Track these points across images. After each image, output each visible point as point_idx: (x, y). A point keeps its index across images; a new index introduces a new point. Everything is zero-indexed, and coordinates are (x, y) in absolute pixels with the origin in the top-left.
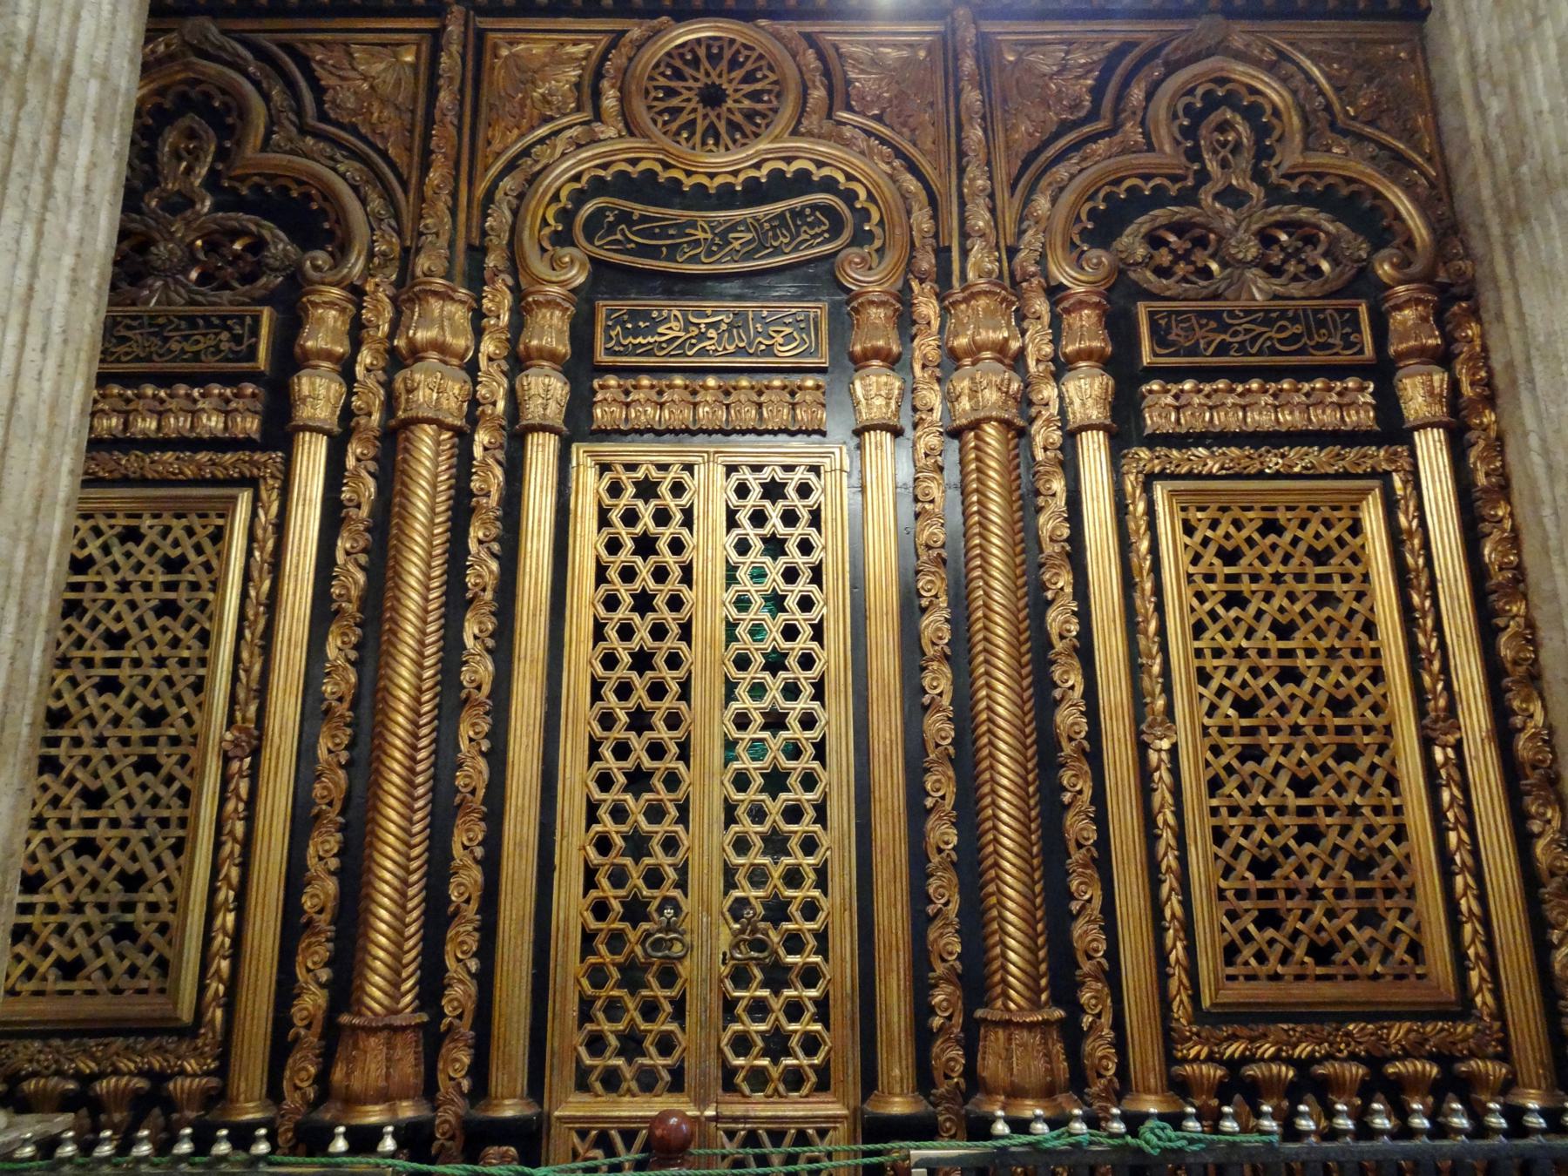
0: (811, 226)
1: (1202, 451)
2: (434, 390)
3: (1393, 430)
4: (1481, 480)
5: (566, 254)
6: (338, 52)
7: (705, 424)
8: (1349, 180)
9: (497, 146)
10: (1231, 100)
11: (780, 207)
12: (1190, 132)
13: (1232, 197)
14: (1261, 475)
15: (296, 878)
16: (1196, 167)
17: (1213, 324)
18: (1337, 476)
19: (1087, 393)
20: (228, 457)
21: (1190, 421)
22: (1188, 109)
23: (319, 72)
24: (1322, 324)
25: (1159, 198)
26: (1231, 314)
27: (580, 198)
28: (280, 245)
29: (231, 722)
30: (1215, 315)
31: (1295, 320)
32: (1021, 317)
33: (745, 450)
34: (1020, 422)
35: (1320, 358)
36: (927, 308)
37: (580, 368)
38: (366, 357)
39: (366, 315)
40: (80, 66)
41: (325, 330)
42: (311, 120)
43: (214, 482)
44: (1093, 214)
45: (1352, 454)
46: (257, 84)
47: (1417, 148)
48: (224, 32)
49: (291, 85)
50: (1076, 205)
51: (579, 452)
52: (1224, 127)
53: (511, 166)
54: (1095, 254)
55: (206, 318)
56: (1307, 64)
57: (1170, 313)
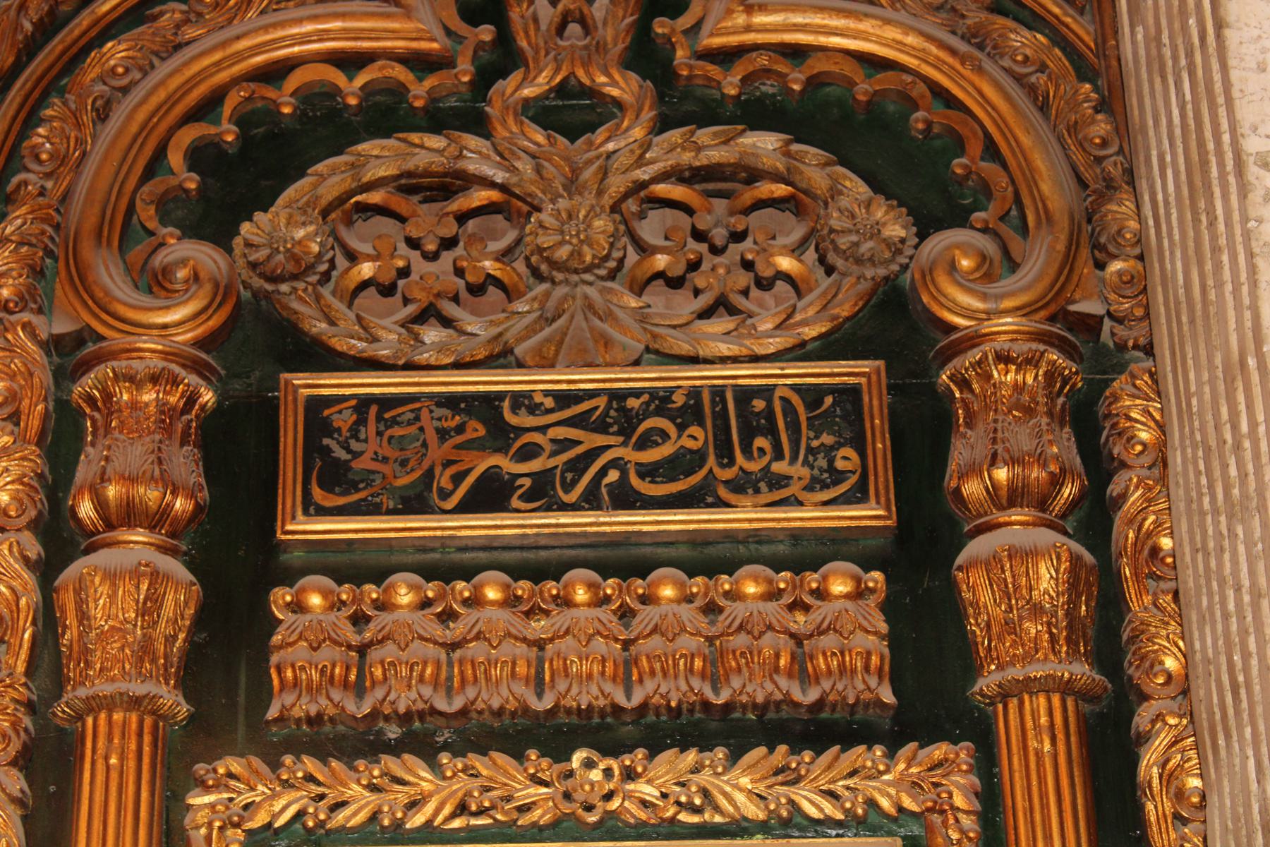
16: (486, 33)
17: (476, 429)
25: (386, 115)
26: (521, 401)
30: (486, 405)
54: (188, 254)
57: (364, 403)
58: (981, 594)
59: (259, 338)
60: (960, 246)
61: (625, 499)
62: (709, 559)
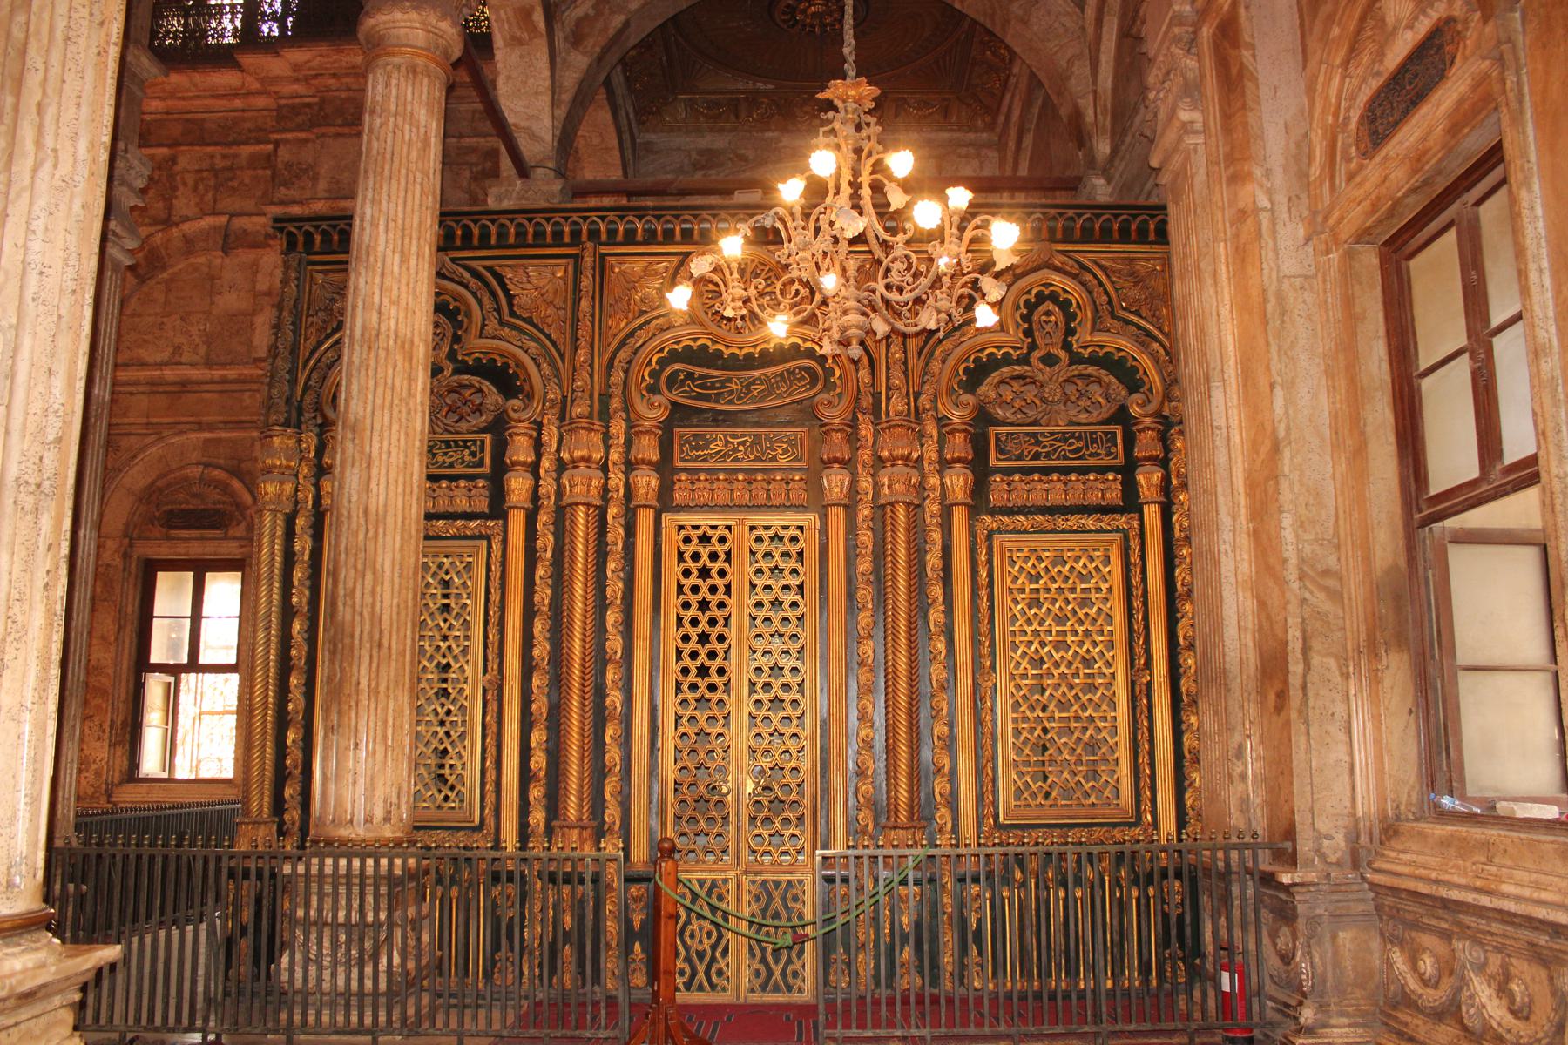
0: (799, 380)
1: (1021, 518)
2: (583, 485)
3: (1131, 503)
4: (1177, 534)
5: (657, 399)
6: (521, 271)
7: (737, 502)
8: (1119, 350)
9: (613, 330)
10: (1053, 297)
11: (782, 367)
12: (1026, 318)
13: (1049, 360)
14: (1054, 531)
15: (525, 752)
18: (1097, 531)
19: (958, 482)
20: (473, 524)
21: (1017, 500)
22: (1027, 302)
23: (510, 286)
24: (1094, 441)
26: (1043, 434)
27: (663, 363)
28: (493, 397)
29: (485, 671)
30: (1034, 435)
31: (1079, 439)
32: (921, 435)
33: (759, 519)
34: (916, 501)
35: (1092, 462)
36: (866, 430)
37: (665, 467)
38: (546, 463)
39: (545, 438)
40: (416, 340)
41: (521, 449)
42: (507, 317)
43: (466, 537)
44: (966, 370)
45: (1106, 518)
46: (474, 294)
47: (1160, 329)
48: (453, 260)
49: (493, 294)
50: (956, 366)
51: (667, 518)
52: (1048, 313)
53: (623, 343)
55: (456, 442)
56: (1100, 274)
58: (1141, 479)
59: (983, 418)
60: (1138, 397)
61: (1065, 458)
62: (1083, 471)
